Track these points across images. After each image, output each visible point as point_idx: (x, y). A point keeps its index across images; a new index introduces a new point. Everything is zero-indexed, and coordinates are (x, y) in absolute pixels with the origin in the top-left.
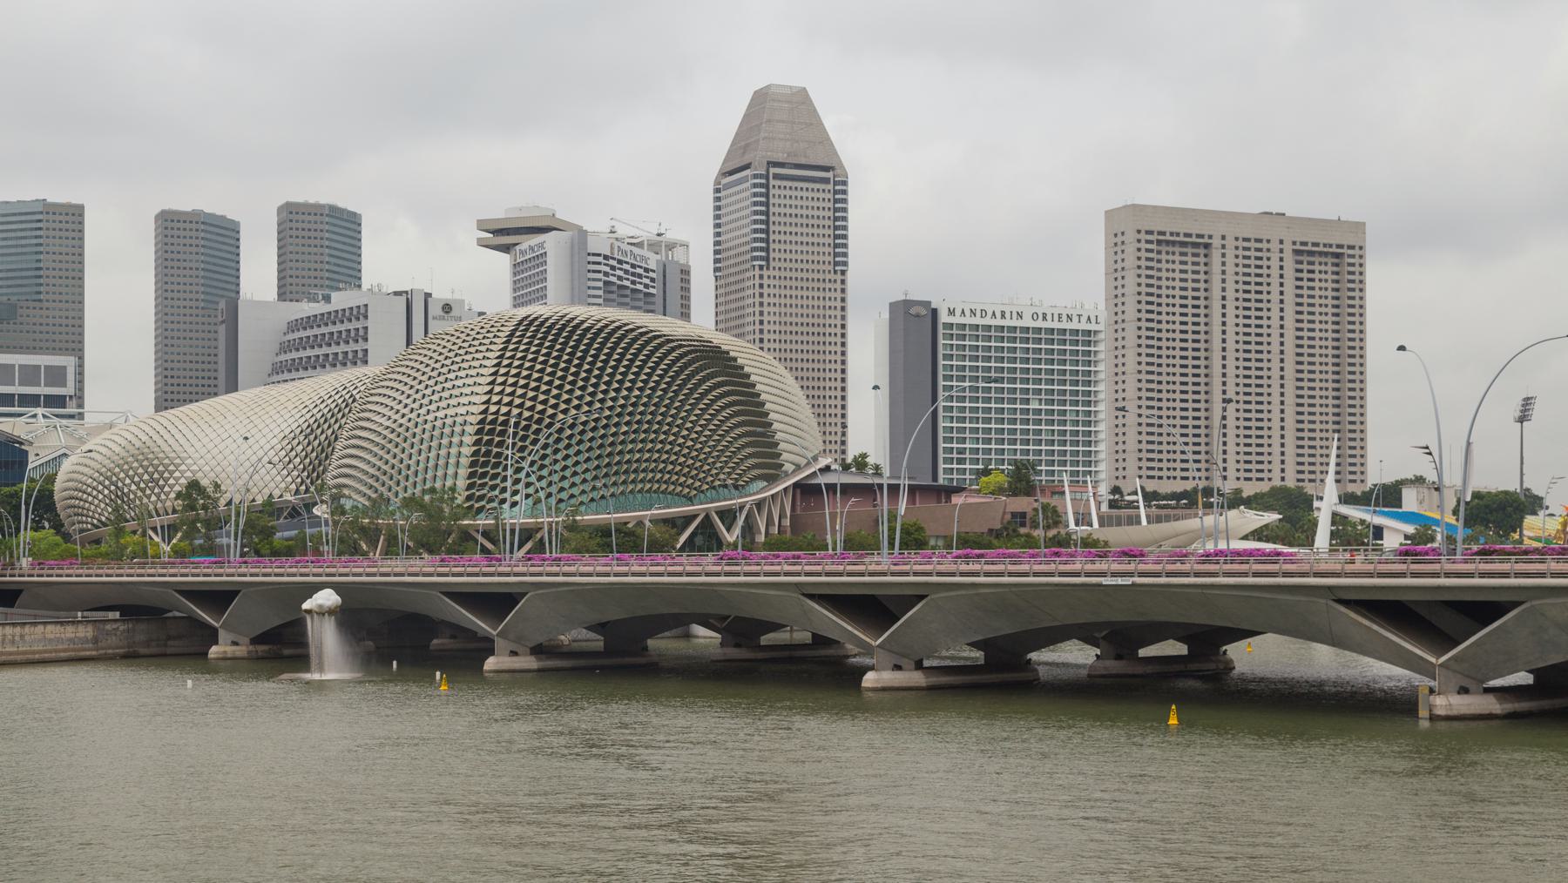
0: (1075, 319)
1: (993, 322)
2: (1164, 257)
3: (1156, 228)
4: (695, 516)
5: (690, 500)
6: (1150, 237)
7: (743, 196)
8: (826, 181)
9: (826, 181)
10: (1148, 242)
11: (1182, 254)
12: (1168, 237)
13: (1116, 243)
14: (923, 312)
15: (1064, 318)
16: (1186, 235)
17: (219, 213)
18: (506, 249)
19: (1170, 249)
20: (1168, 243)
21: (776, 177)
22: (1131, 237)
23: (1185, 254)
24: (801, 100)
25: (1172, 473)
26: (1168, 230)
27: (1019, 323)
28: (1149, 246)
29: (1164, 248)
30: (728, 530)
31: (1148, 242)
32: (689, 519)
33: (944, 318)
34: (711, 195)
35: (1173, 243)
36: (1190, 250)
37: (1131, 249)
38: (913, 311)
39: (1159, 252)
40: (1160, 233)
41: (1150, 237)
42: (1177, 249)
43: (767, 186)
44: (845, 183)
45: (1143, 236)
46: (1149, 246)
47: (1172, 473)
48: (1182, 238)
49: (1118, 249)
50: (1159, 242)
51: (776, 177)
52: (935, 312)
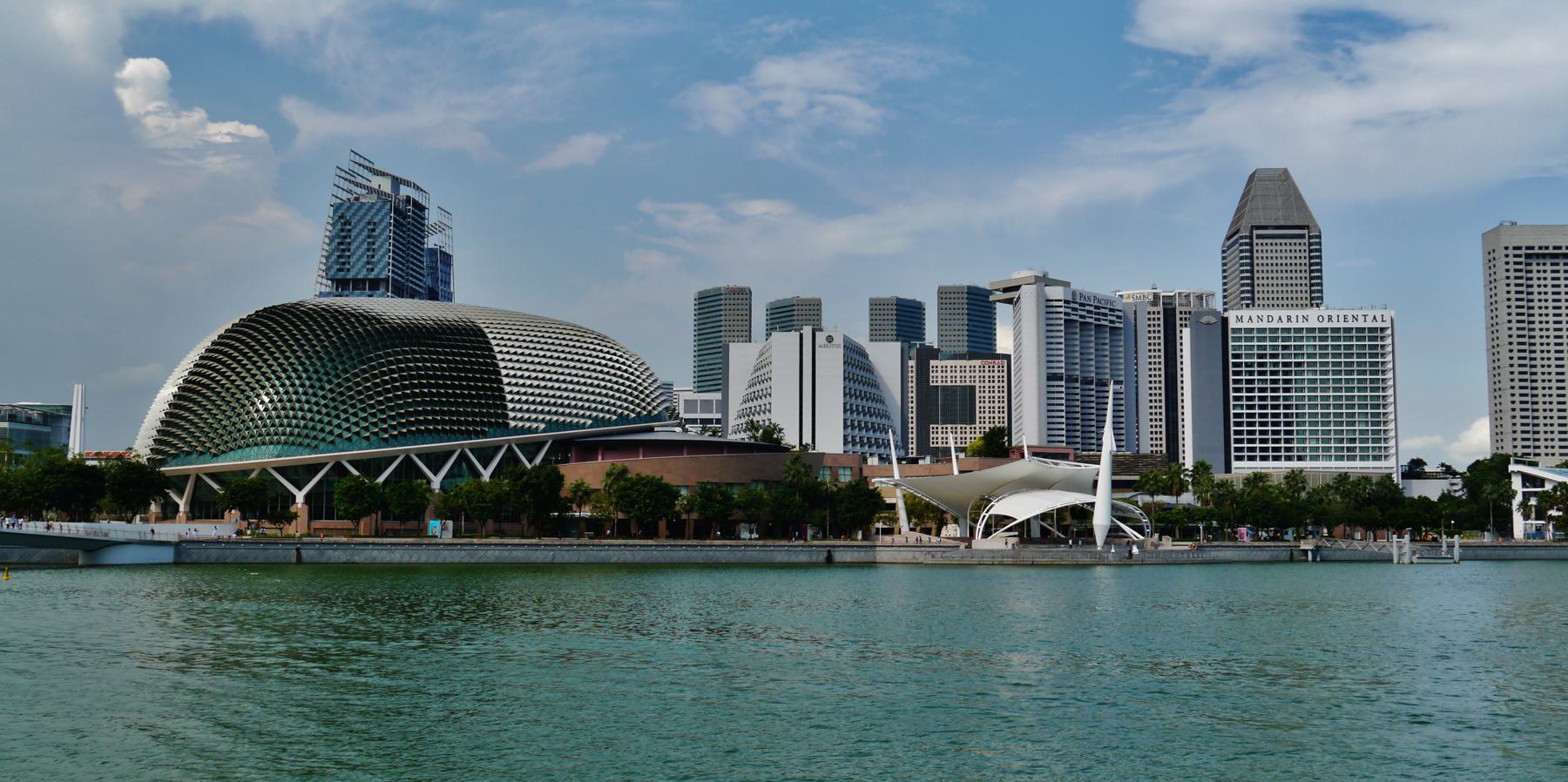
0: (1361, 319)
1: (1280, 326)
3: (1524, 244)
4: (324, 465)
5: (315, 449)
7: (1234, 253)
8: (1302, 236)
9: (1302, 236)
12: (1536, 251)
13: (1490, 261)
14: (1213, 320)
15: (1350, 318)
17: (909, 297)
18: (1009, 301)
20: (1538, 256)
21: (1259, 237)
22: (1501, 252)
24: (1283, 178)
25: (1550, 451)
26: (1536, 245)
27: (1305, 325)
33: (1232, 324)
34: (1219, 255)
35: (1544, 256)
38: (1204, 319)
42: (1548, 262)
43: (1251, 244)
44: (1319, 237)
45: (1511, 252)
47: (1550, 451)
48: (1551, 251)
50: (1527, 256)
51: (1259, 237)
52: (1225, 321)
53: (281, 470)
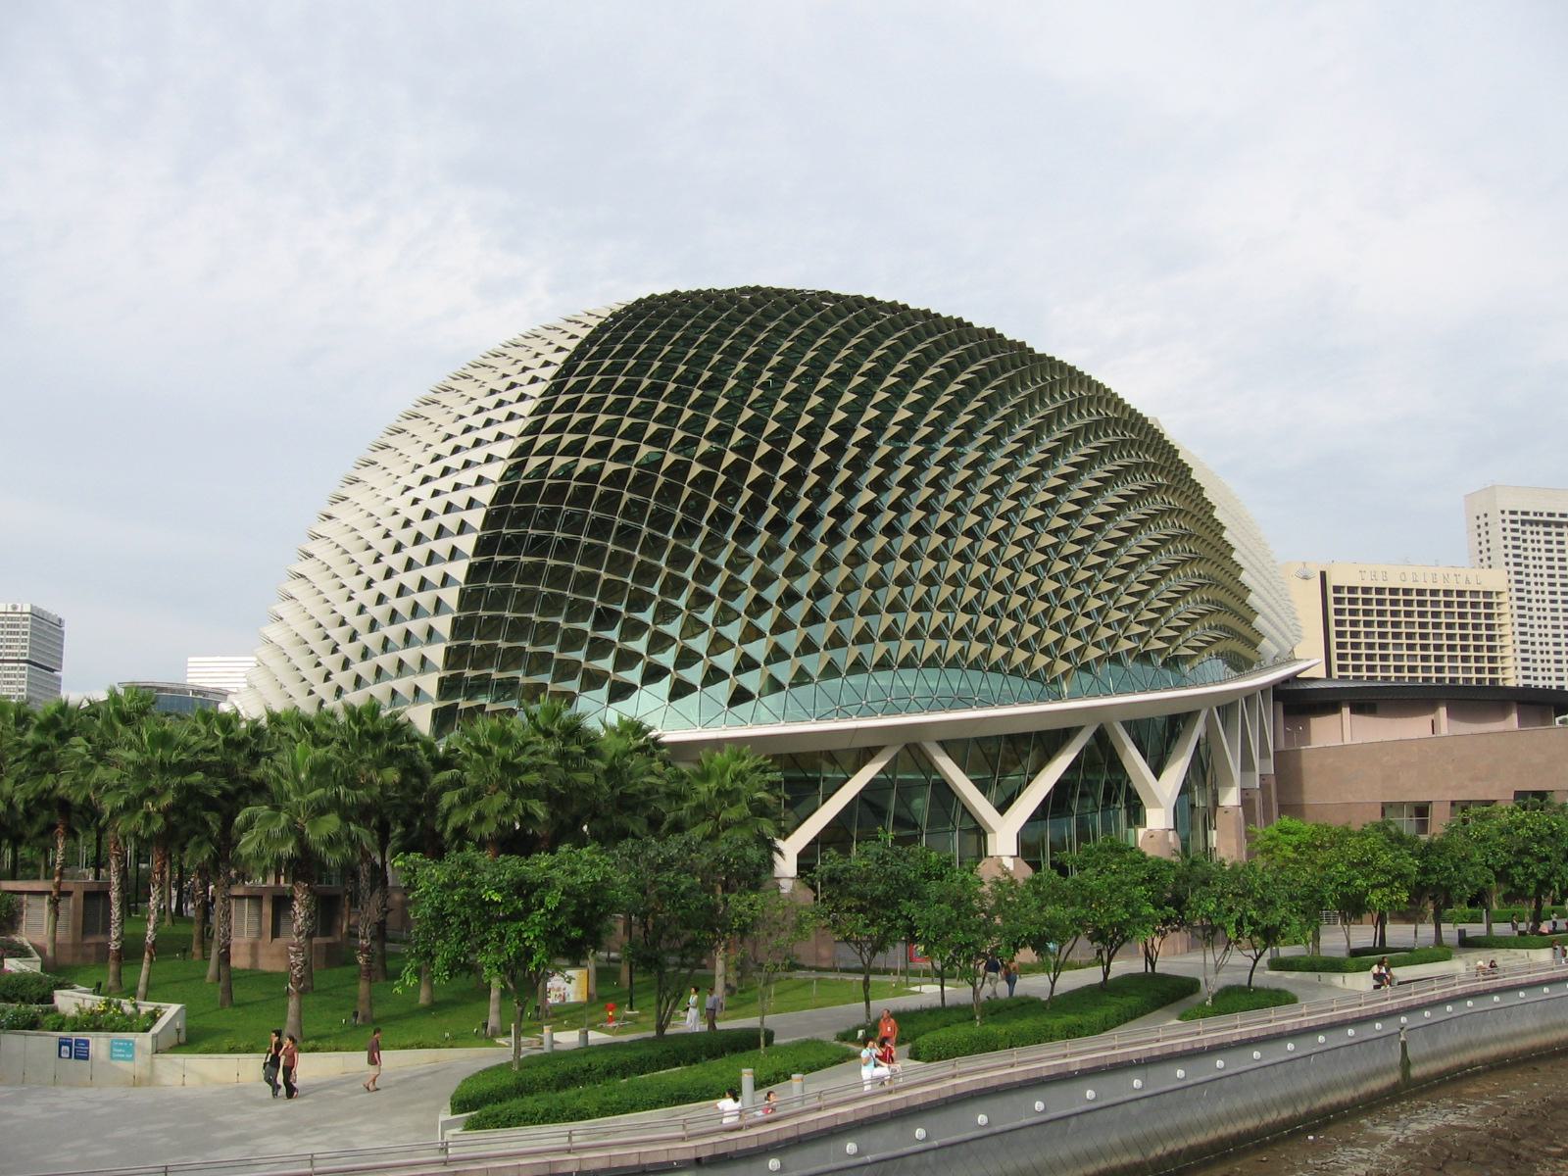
2: (1528, 536)
3: (1520, 509)
6: (1514, 517)
10: (1513, 522)
11: (1546, 534)
12: (1531, 517)
16: (1550, 515)
19: (1535, 528)
20: (1531, 523)
22: (1495, 518)
23: (1549, 534)
28: (1515, 526)
29: (1528, 528)
30: (1157, 772)
31: (1513, 522)
32: (1049, 741)
33: (1332, 582)
35: (1537, 523)
36: (1553, 529)
37: (1496, 531)
39: (1524, 532)
40: (1524, 513)
41: (1514, 517)
42: (1541, 529)
45: (1508, 517)
46: (1515, 526)
48: (1545, 518)
49: (1482, 531)
50: (1523, 523)
52: (1323, 575)
53: (960, 746)
